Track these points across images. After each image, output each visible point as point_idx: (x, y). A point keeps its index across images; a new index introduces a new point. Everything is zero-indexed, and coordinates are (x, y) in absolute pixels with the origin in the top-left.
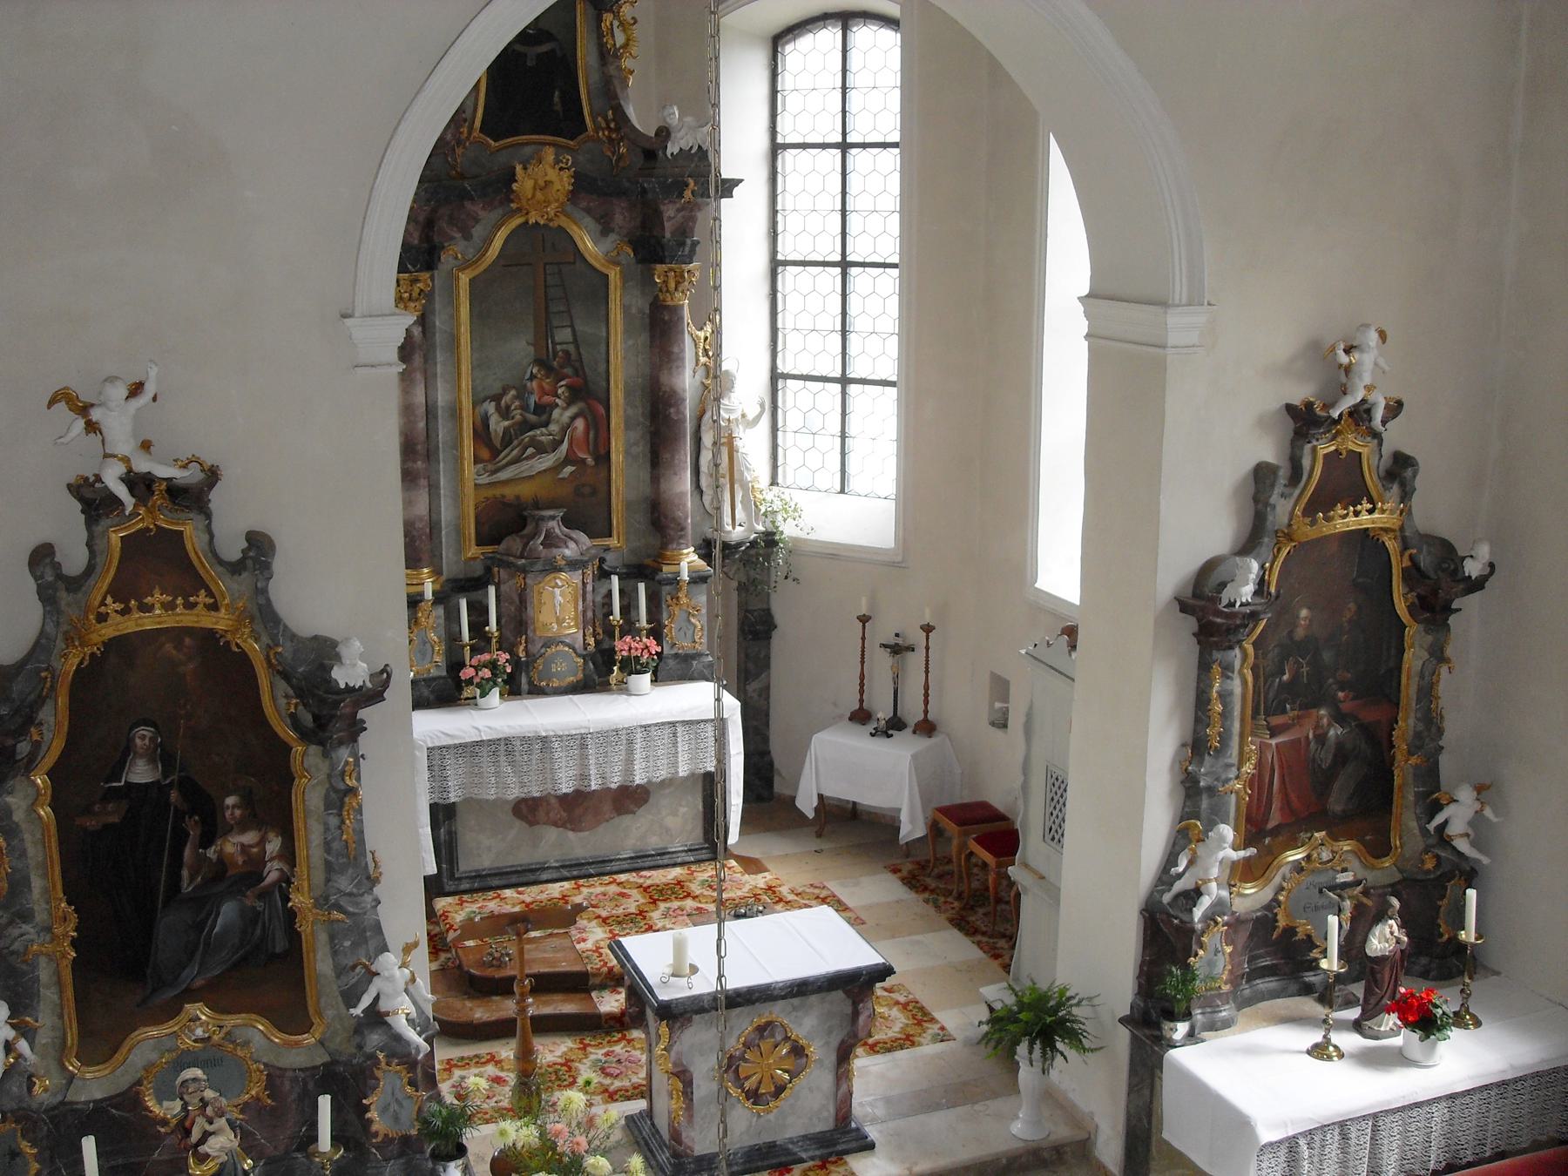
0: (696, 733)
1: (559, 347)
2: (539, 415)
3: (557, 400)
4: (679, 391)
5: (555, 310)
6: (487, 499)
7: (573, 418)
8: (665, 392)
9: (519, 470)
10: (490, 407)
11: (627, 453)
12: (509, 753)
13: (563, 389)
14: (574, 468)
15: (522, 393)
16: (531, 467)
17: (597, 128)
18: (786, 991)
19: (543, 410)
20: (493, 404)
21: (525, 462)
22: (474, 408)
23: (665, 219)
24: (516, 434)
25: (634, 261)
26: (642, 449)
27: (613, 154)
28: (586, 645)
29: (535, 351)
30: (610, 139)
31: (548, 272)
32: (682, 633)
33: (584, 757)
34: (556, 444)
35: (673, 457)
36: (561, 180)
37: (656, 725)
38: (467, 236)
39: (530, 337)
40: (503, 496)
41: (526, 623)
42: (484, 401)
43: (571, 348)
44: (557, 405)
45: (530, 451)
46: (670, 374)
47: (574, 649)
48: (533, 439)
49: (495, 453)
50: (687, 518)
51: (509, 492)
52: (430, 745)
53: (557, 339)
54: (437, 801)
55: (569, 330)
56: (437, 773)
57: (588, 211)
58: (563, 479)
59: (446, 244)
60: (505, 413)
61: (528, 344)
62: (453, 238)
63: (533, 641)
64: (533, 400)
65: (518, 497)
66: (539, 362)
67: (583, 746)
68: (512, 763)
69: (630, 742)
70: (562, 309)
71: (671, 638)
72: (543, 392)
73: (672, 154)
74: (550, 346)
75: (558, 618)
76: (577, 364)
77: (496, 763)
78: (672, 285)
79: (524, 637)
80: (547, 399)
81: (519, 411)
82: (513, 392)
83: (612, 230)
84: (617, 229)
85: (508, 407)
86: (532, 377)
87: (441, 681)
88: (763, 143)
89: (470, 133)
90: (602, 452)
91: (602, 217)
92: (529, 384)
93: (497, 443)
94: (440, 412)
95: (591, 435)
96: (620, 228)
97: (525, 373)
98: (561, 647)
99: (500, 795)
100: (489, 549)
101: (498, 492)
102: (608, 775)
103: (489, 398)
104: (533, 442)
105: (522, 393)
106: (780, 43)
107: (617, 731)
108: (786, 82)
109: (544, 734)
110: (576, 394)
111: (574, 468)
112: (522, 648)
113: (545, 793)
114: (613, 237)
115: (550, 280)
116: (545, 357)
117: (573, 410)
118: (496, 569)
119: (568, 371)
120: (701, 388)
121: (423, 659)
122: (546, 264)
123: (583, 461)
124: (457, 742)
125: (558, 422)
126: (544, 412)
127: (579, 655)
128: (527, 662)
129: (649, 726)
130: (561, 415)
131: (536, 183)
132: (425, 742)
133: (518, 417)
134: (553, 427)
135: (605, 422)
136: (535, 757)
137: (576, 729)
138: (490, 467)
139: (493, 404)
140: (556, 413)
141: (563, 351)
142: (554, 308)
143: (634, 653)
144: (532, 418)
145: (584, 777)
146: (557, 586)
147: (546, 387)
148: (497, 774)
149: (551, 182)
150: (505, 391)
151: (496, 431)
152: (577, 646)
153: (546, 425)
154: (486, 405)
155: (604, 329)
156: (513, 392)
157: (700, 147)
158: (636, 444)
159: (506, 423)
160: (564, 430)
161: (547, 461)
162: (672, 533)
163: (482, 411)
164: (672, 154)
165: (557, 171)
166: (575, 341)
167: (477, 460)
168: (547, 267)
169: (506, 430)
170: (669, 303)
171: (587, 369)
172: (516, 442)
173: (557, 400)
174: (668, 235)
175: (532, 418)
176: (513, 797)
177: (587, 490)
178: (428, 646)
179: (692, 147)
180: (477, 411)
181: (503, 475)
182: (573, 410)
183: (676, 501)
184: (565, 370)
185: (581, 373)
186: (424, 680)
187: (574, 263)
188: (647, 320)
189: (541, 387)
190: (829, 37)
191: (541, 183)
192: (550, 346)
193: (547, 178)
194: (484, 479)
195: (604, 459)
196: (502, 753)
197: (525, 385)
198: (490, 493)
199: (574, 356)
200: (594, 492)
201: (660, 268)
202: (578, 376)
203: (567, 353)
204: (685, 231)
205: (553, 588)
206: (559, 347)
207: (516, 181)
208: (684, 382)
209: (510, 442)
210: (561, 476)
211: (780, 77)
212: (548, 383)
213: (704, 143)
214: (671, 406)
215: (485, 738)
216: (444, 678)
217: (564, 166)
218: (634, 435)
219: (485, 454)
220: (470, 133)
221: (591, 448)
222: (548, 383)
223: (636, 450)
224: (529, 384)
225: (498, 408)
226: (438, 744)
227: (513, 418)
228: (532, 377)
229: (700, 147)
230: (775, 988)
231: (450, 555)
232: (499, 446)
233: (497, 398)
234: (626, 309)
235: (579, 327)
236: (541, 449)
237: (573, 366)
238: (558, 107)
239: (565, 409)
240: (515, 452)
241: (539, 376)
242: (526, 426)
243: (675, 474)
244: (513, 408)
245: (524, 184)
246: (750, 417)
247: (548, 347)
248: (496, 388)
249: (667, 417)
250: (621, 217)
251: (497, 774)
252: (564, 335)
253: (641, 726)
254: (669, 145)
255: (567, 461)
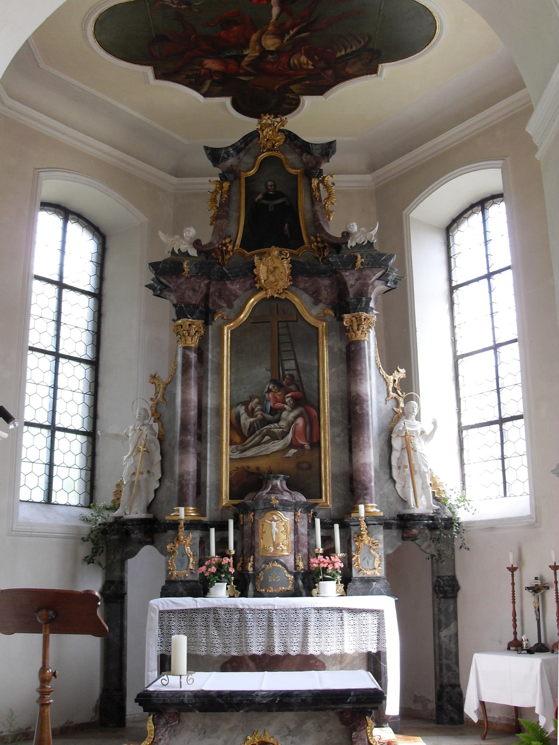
0: (359, 619)
1: (286, 372)
2: (273, 415)
3: (285, 406)
4: (364, 396)
5: (285, 349)
6: (238, 468)
7: (296, 418)
8: (354, 396)
9: (259, 451)
10: (242, 409)
11: (332, 441)
12: (217, 620)
13: (289, 399)
14: (296, 451)
15: (262, 401)
16: (268, 449)
17: (311, 243)
18: (268, 699)
19: (276, 412)
20: (243, 407)
21: (263, 446)
22: (231, 410)
23: (349, 286)
24: (258, 426)
25: (335, 319)
26: (342, 439)
27: (320, 256)
28: (296, 566)
29: (271, 374)
30: (319, 248)
31: (280, 327)
32: (365, 562)
33: (270, 627)
34: (284, 434)
35: (358, 439)
36: (283, 266)
37: (327, 609)
38: (230, 306)
39: (268, 366)
40: (249, 467)
41: (254, 547)
42: (238, 405)
43: (295, 373)
44: (285, 409)
45: (267, 438)
46: (356, 384)
47: (285, 566)
48: (269, 430)
49: (244, 438)
50: (371, 481)
51: (252, 464)
52: (161, 609)
53: (286, 367)
54: (164, 652)
55: (293, 362)
56: (165, 631)
57: (305, 290)
58: (289, 457)
59: (217, 311)
60: (251, 413)
61: (267, 370)
62: (221, 307)
63: (258, 560)
64: (269, 405)
65: (258, 469)
66: (273, 381)
67: (270, 620)
68: (218, 628)
69: (306, 620)
70: (289, 349)
71: (358, 565)
72: (276, 400)
73: (351, 247)
74: (281, 371)
75: (274, 543)
76: (298, 383)
77: (207, 627)
78: (355, 327)
79: (252, 557)
80: (279, 405)
81: (260, 412)
82: (256, 400)
83: (320, 301)
84: (323, 301)
85: (253, 409)
86: (269, 391)
87: (194, 584)
88: (445, 287)
89: (233, 247)
90: (315, 440)
91: (313, 294)
92: (267, 395)
93: (245, 432)
94: (209, 412)
95: (308, 428)
96: (325, 299)
97: (265, 388)
98: (276, 564)
99: (208, 653)
100: (237, 502)
101: (245, 464)
102: (289, 644)
103: (241, 403)
104: (269, 433)
105: (262, 401)
106: (451, 230)
107: (295, 610)
108: (455, 250)
109: (241, 607)
110: (297, 402)
111: (296, 451)
112: (250, 564)
113: (241, 654)
114: (321, 305)
115: (281, 331)
116: (277, 378)
117: (296, 412)
118: (242, 515)
119: (292, 387)
120: (392, 414)
121: (182, 567)
122: (278, 322)
123: (302, 446)
124: (180, 608)
125: (285, 420)
126: (277, 414)
127: (290, 573)
128: (254, 574)
129: (321, 609)
130: (288, 415)
131: (268, 268)
132: (158, 606)
133: (259, 416)
134: (283, 423)
135: (317, 419)
136: (234, 624)
137: (264, 605)
138: (240, 447)
139: (243, 407)
140: (284, 414)
141: (289, 374)
142: (284, 348)
143: (322, 565)
144: (269, 417)
145: (270, 646)
146: (273, 520)
147: (278, 397)
148: (207, 635)
149: (277, 267)
150: (251, 399)
151: (244, 424)
152: (288, 565)
153: (278, 421)
154: (239, 407)
155: (316, 362)
156: (256, 400)
157: (368, 242)
158: (339, 436)
159: (252, 420)
160: (290, 425)
161: (278, 445)
162: (359, 491)
163: (236, 411)
164: (351, 247)
165: (280, 260)
166: (297, 369)
167: (232, 443)
168: (279, 323)
169: (251, 424)
170: (354, 339)
171: (304, 386)
172: (257, 432)
173: (285, 406)
174: (351, 296)
175: (269, 417)
176: (218, 654)
177: (305, 466)
178: (185, 557)
179: (363, 242)
180: (233, 411)
181: (249, 453)
182: (296, 412)
183: (362, 469)
184: (291, 387)
185: (301, 389)
186: (181, 581)
187: (297, 321)
188: (345, 356)
189: (275, 398)
190: (476, 218)
191: (271, 268)
192: (281, 371)
193: (275, 265)
194: (237, 456)
195: (316, 445)
196: (211, 619)
197: (265, 396)
198: (240, 465)
199: (296, 378)
200: (310, 467)
201: (346, 316)
202: (299, 390)
203: (292, 376)
204: (362, 293)
205: (271, 521)
206: (286, 372)
207: (256, 267)
208: (366, 390)
209: (254, 432)
210: (287, 456)
211: (452, 248)
212: (279, 395)
213: (371, 239)
214: (356, 404)
215: (199, 607)
216: (196, 581)
217: (284, 257)
218: (337, 430)
219: (237, 439)
220: (233, 247)
221: (308, 438)
222: (279, 395)
223: (338, 440)
224: (267, 395)
225: (247, 410)
226: (166, 608)
227: (256, 416)
228: (269, 391)
229: (368, 242)
230: (257, 695)
231: (212, 505)
232: (247, 436)
233: (245, 404)
234: (330, 349)
235: (300, 360)
236: (275, 437)
237: (296, 385)
238: (287, 233)
239: (290, 412)
240: (257, 438)
241: (273, 390)
242: (264, 422)
243: (361, 450)
244: (256, 410)
245: (262, 271)
246: (428, 432)
247: (279, 373)
248: (246, 397)
249: (355, 412)
250: (326, 292)
251: (207, 635)
252: (290, 365)
253: (315, 609)
254: (349, 241)
255: (292, 445)
